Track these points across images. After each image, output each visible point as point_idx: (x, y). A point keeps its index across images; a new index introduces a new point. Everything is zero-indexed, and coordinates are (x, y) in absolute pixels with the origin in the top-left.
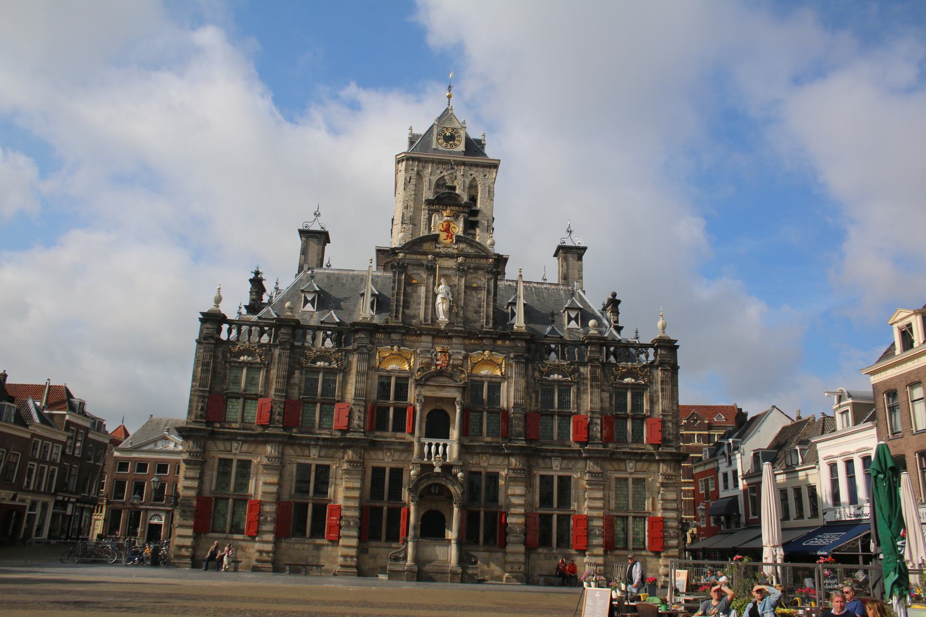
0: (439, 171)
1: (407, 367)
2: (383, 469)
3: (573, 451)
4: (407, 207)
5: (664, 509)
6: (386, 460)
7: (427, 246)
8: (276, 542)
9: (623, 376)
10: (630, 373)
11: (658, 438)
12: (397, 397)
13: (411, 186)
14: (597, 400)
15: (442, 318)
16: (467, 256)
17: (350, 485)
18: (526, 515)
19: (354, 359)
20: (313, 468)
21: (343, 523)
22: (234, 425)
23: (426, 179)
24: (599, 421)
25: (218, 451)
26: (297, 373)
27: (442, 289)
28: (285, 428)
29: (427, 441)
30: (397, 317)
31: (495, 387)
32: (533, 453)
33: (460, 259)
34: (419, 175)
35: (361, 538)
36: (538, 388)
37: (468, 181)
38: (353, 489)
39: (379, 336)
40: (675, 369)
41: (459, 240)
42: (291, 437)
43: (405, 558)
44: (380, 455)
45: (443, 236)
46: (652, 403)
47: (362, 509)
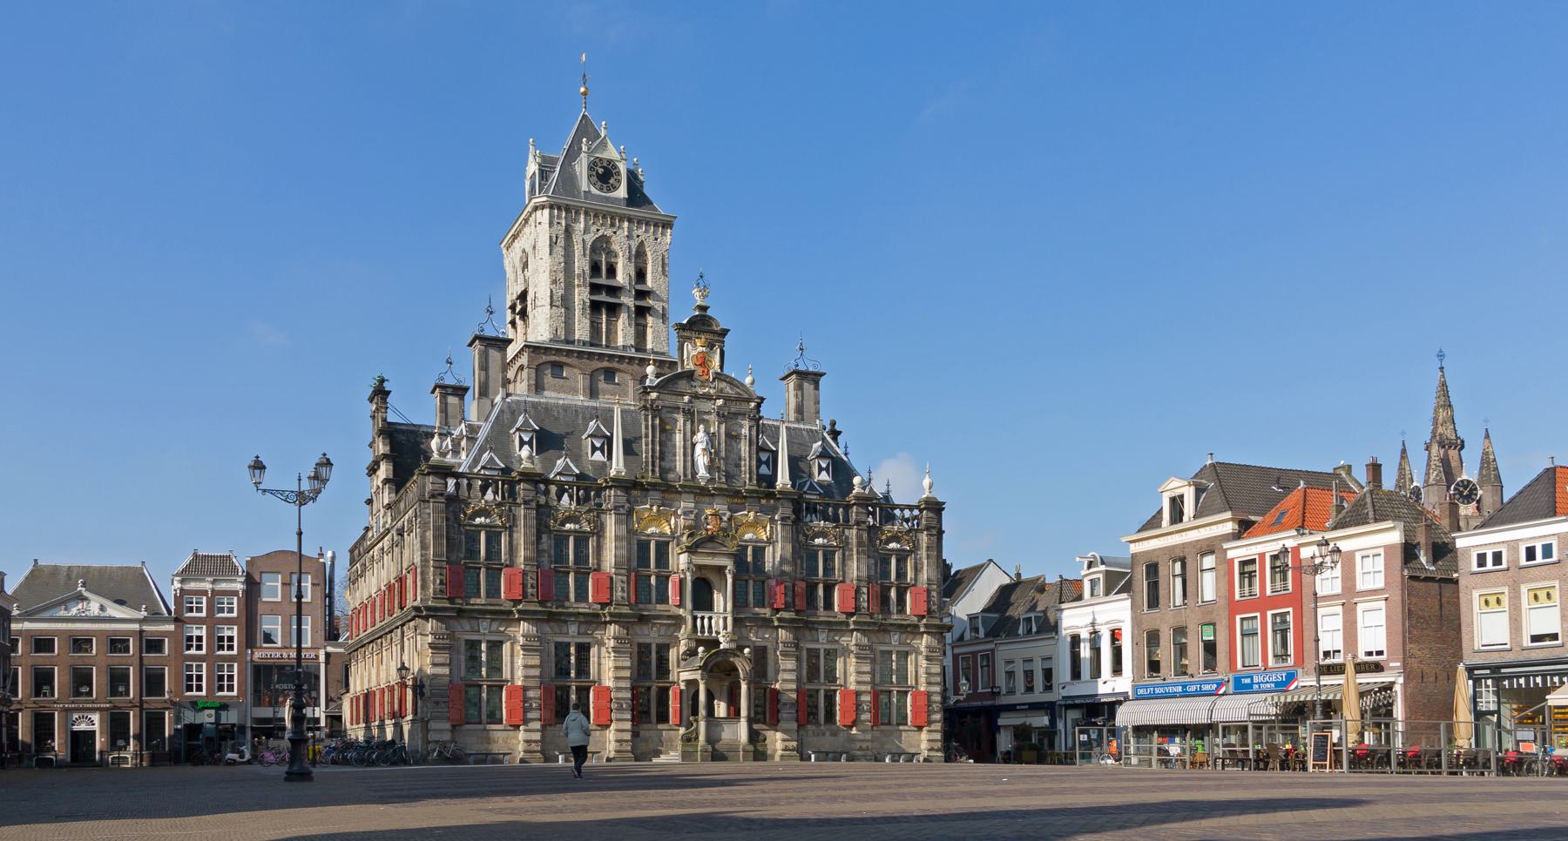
0: (594, 228)
2: (649, 645)
3: (841, 623)
4: (554, 282)
5: (929, 683)
6: (652, 636)
7: (683, 385)
8: (543, 730)
9: (889, 541)
10: (895, 538)
11: (923, 610)
12: (657, 566)
13: (559, 250)
14: (864, 568)
15: (702, 472)
16: (727, 399)
17: (620, 664)
18: (797, 691)
19: (610, 522)
21: (614, 706)
23: (577, 238)
25: (465, 632)
26: (545, 537)
27: (700, 436)
28: (541, 603)
31: (759, 552)
32: (802, 627)
33: (720, 402)
34: (568, 232)
35: (633, 720)
36: (803, 552)
37: (634, 244)
38: (623, 668)
39: (634, 493)
40: (940, 533)
41: (719, 377)
42: (550, 613)
43: (697, 738)
44: (645, 629)
45: (699, 370)
46: (917, 570)
47: (633, 689)
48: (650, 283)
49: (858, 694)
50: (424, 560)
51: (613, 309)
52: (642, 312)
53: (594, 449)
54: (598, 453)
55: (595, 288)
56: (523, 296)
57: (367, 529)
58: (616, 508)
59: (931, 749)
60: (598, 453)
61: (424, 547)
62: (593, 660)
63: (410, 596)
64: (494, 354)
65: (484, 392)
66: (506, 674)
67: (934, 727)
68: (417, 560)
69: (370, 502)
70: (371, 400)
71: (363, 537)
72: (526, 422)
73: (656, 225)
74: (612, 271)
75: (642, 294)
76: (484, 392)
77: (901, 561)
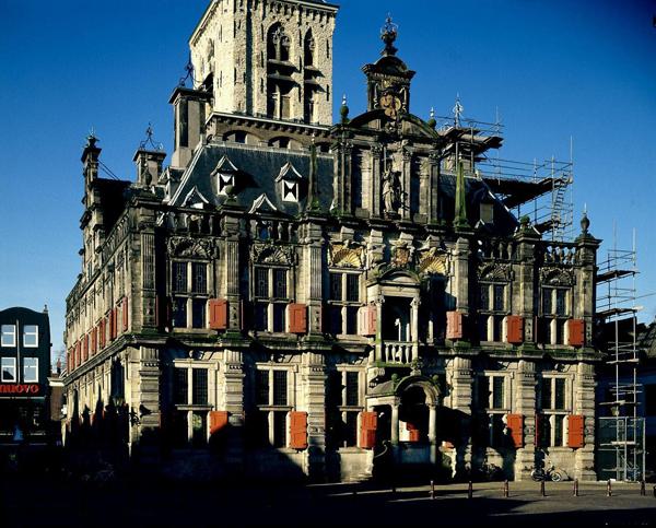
0: (271, 15)
1: (357, 264)
4: (238, 62)
13: (242, 34)
17: (315, 391)
19: (307, 255)
20: (271, 375)
22: (185, 331)
24: (531, 322)
29: (388, 344)
30: (345, 208)
48: (316, 65)
49: (524, 417)
50: (134, 291)
51: (287, 86)
52: (310, 89)
53: (287, 190)
54: (290, 194)
55: (271, 68)
56: (209, 81)
57: (81, 277)
58: (312, 241)
59: (586, 468)
60: (290, 194)
61: (134, 277)
62: (290, 388)
63: (120, 327)
64: (194, 106)
65: (184, 143)
66: (211, 400)
67: (586, 449)
68: (128, 291)
69: (83, 252)
70: (83, 160)
71: (78, 283)
72: (226, 163)
73: (322, 15)
74: (285, 55)
75: (310, 74)
76: (184, 143)
77: (561, 296)
